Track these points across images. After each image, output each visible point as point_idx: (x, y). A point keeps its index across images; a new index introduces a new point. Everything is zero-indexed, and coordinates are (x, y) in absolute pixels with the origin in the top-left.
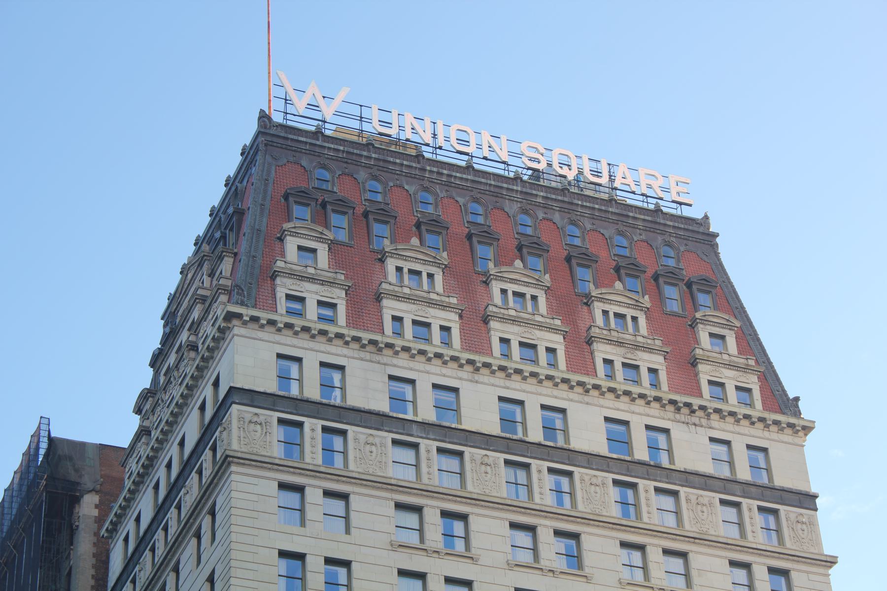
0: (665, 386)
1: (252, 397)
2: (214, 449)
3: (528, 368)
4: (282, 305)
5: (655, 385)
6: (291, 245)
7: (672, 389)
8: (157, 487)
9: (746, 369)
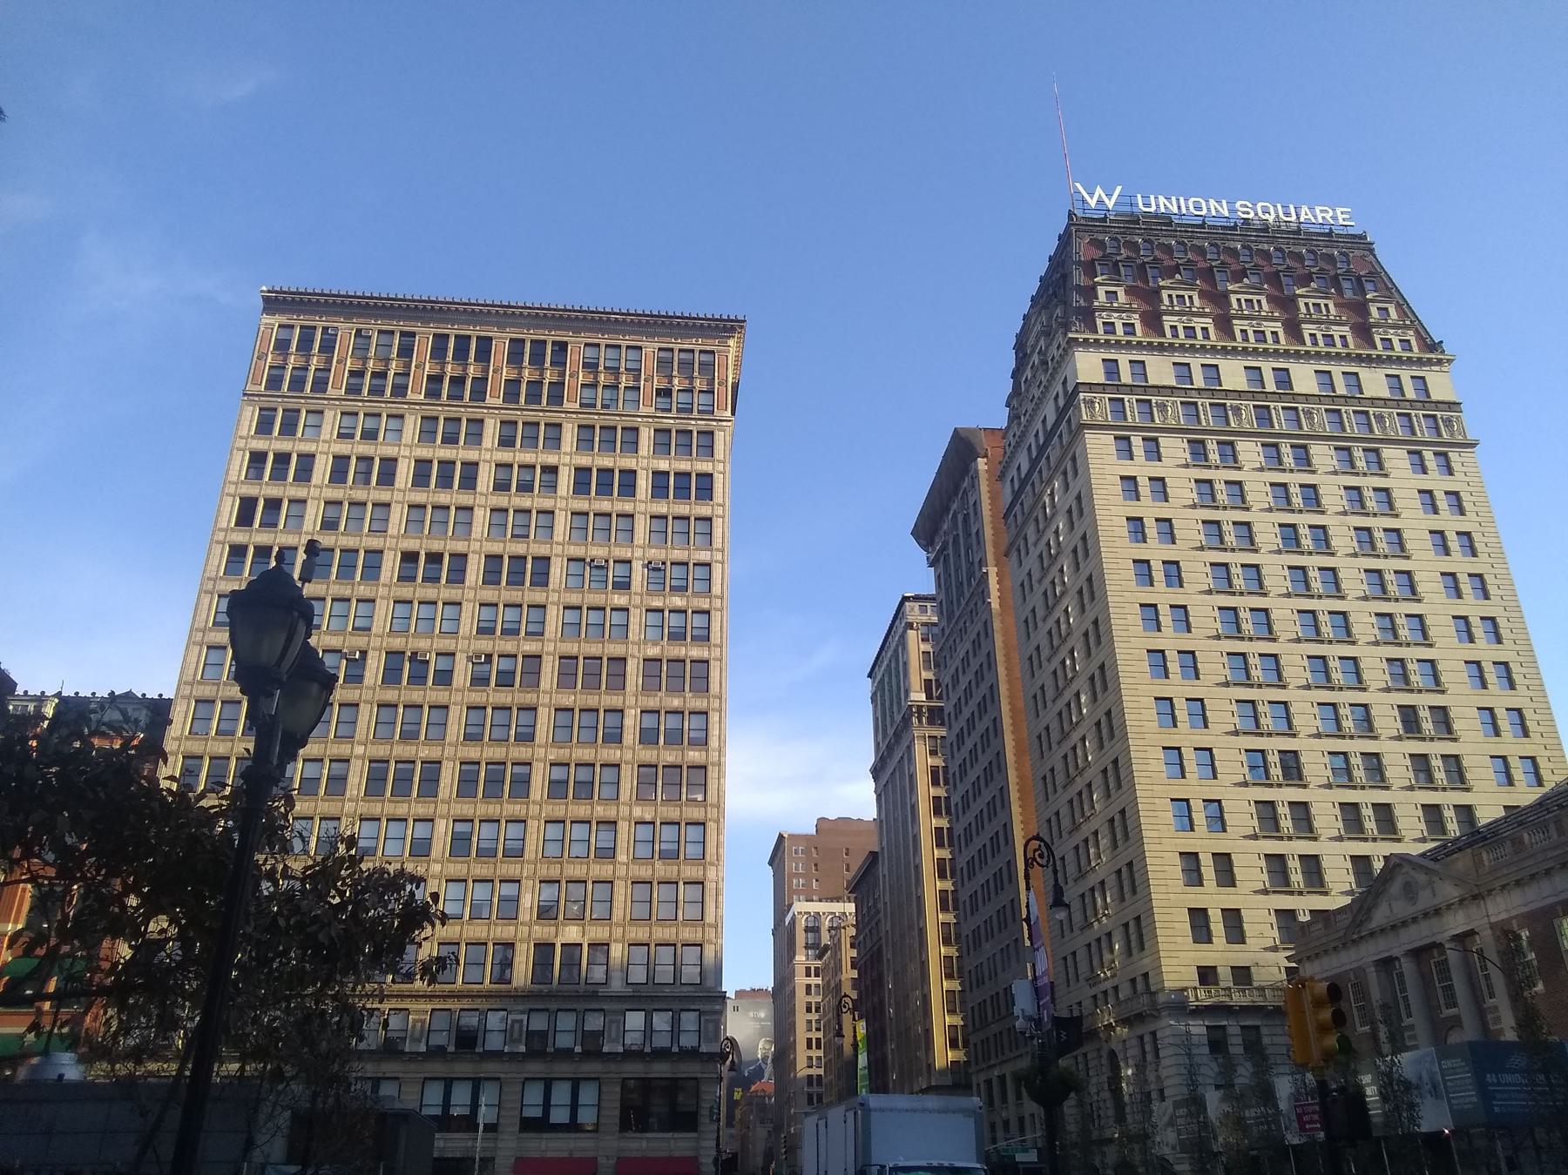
0: (1352, 346)
1: (1091, 387)
2: (1069, 421)
3: (1261, 346)
4: (1101, 329)
5: (1345, 345)
6: (1101, 291)
7: (1358, 346)
8: (1029, 448)
9: (1406, 327)
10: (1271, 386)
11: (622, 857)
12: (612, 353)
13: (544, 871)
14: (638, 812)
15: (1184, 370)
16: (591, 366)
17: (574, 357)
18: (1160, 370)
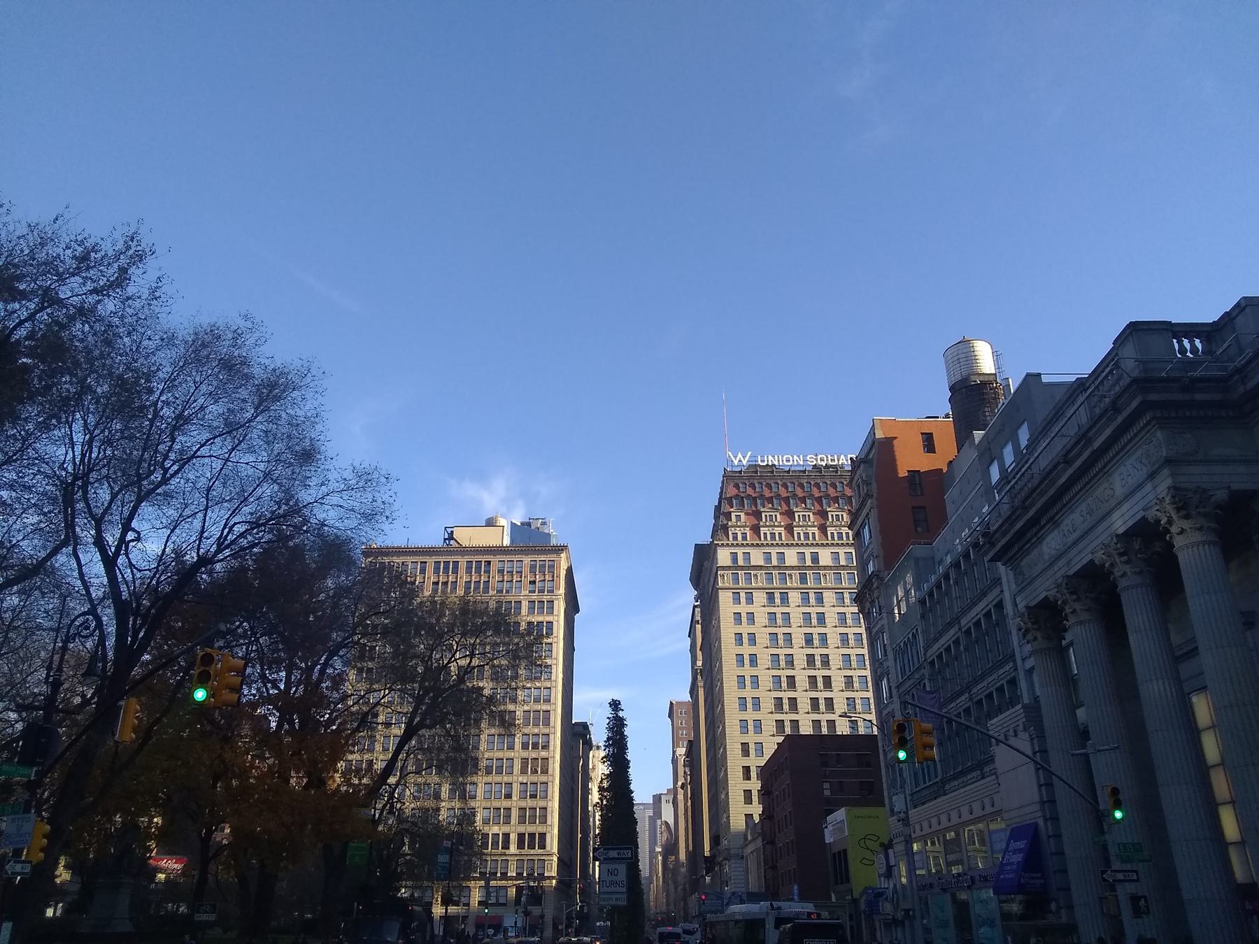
1: (723, 568)
10: (809, 563)
11: (514, 798)
12: (510, 564)
13: (484, 805)
14: (520, 779)
15: (768, 557)
16: (501, 571)
17: (494, 568)
18: (757, 558)
